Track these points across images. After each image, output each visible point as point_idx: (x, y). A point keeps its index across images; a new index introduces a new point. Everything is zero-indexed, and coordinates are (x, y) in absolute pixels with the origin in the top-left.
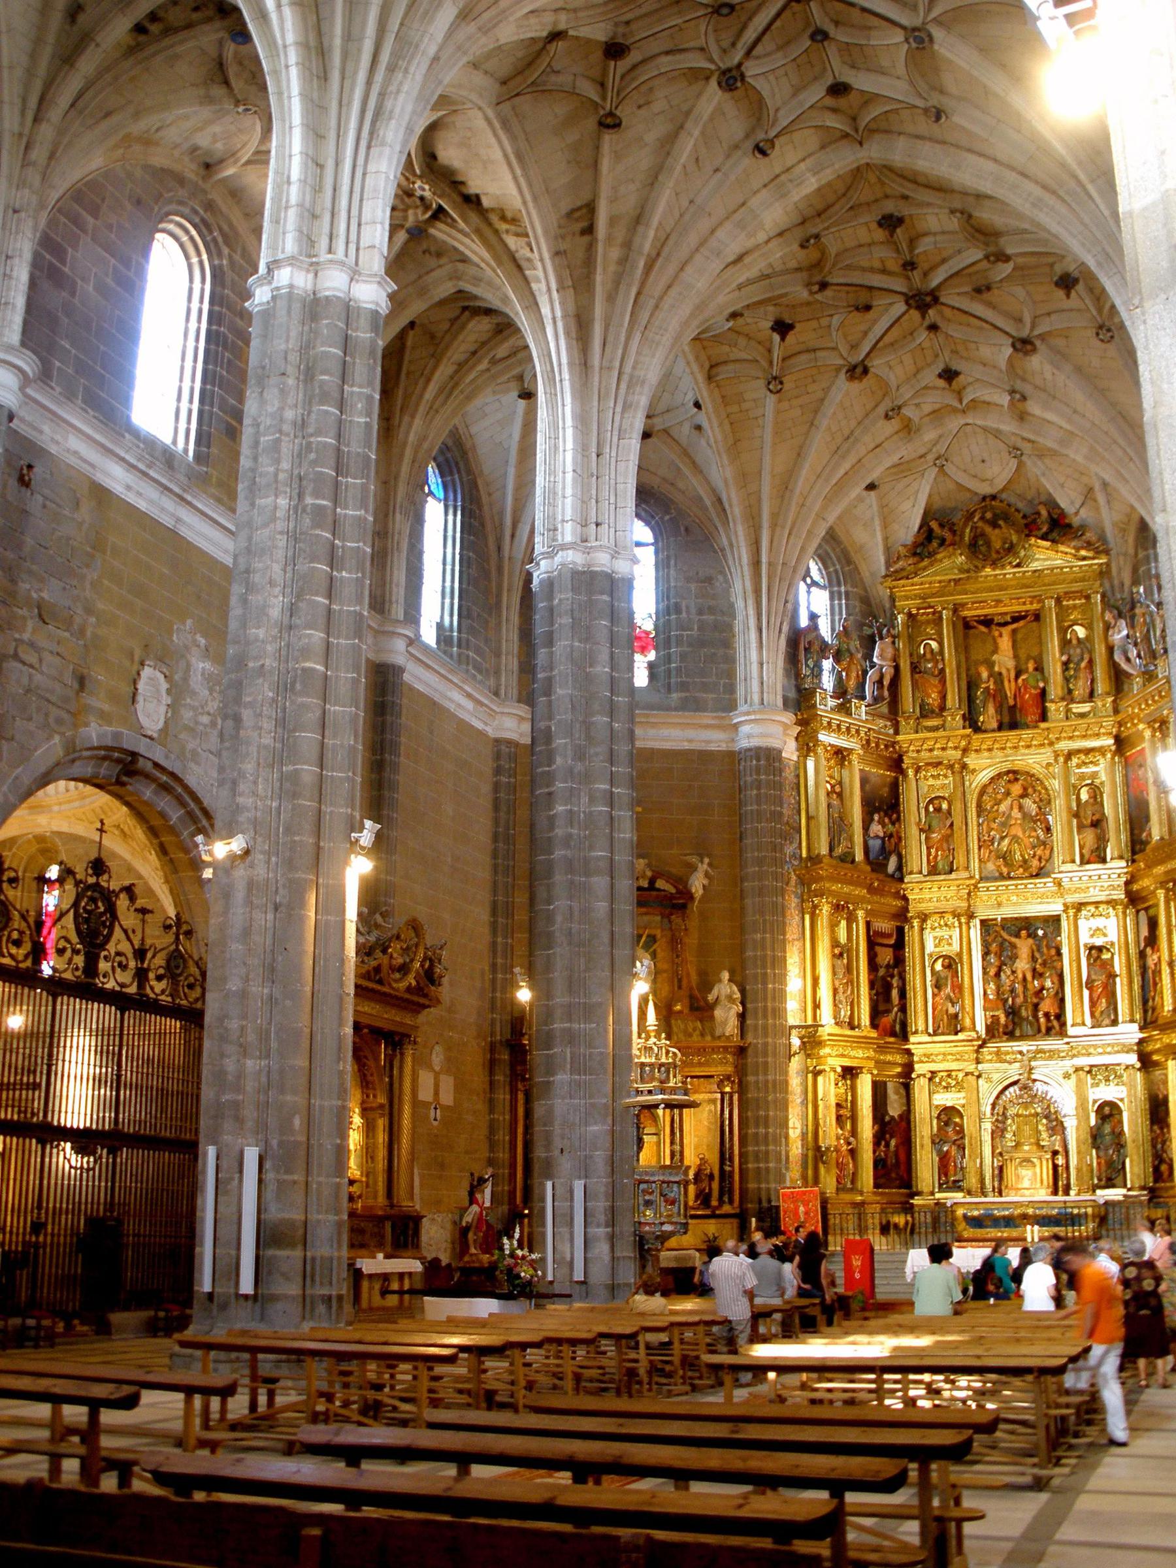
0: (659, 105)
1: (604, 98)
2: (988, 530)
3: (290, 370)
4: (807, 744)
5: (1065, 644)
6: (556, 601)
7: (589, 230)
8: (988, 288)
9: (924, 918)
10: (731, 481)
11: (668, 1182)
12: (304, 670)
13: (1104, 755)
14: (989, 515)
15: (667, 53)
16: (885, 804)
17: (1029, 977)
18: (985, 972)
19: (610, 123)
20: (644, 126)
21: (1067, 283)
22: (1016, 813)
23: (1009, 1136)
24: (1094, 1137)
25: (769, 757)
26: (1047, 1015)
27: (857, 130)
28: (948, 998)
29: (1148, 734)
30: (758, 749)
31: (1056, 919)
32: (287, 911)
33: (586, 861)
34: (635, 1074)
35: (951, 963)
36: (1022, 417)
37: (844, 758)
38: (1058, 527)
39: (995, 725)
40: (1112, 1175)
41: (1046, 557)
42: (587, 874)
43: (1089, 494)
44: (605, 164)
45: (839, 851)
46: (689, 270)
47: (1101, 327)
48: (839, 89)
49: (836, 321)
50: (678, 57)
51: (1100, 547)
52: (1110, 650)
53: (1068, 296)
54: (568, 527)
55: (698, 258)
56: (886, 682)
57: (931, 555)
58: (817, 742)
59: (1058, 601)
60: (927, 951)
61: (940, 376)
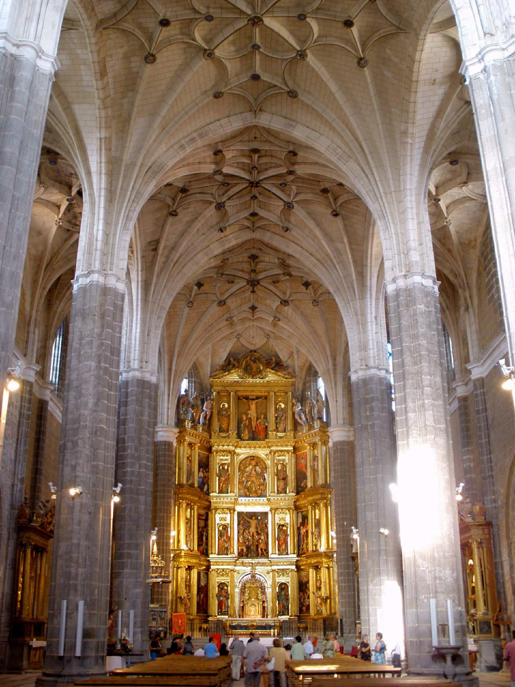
0: (190, 210)
1: (174, 205)
2: (252, 363)
3: (96, 314)
4: (180, 440)
5: (276, 410)
6: (130, 390)
7: (155, 250)
8: (278, 282)
9: (216, 509)
10: (165, 337)
11: (161, 612)
12: (101, 427)
13: (288, 453)
14: (253, 358)
15: (200, 193)
16: (205, 465)
17: (255, 534)
18: (238, 532)
19: (174, 214)
20: (184, 216)
21: (307, 284)
22: (253, 472)
23: (246, 594)
24: (278, 597)
25: (169, 444)
26: (261, 550)
27: (253, 226)
28: (225, 541)
29: (308, 447)
30: (165, 442)
31: (266, 514)
32: (93, 515)
33: (138, 490)
34: (150, 571)
35: (225, 527)
36: (275, 325)
37: (192, 447)
38: (278, 365)
39: (247, 438)
40: (284, 611)
41: (271, 377)
42: (138, 494)
43: (291, 355)
44: (167, 228)
45: (189, 483)
46: (186, 268)
47: (314, 301)
48: (254, 214)
49: (218, 285)
50: (204, 195)
51: (293, 375)
52: (294, 414)
53: (307, 289)
54: (136, 362)
55: (189, 264)
56: (208, 417)
57: (229, 371)
58: (185, 440)
59: (275, 393)
61: (250, 308)
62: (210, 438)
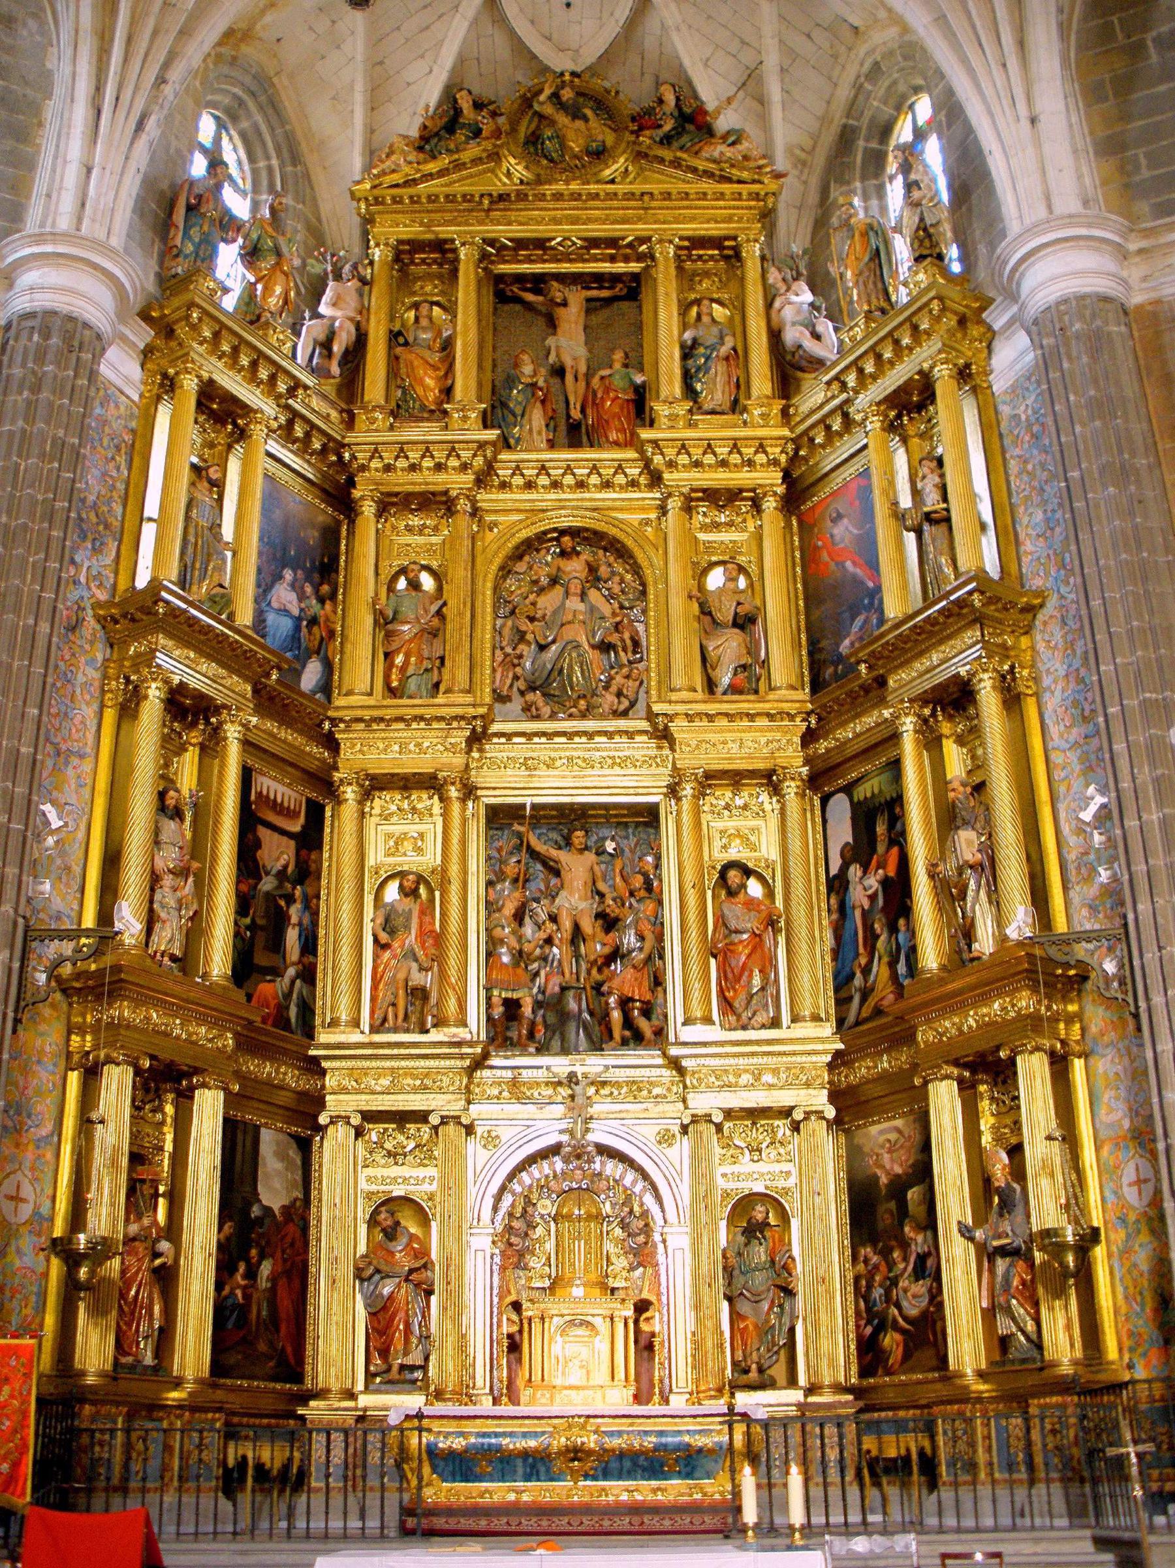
2: (562, 119)
17: (588, 925)
60: (370, 861)
62: (350, 422)
